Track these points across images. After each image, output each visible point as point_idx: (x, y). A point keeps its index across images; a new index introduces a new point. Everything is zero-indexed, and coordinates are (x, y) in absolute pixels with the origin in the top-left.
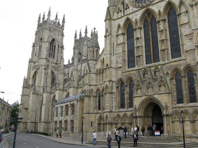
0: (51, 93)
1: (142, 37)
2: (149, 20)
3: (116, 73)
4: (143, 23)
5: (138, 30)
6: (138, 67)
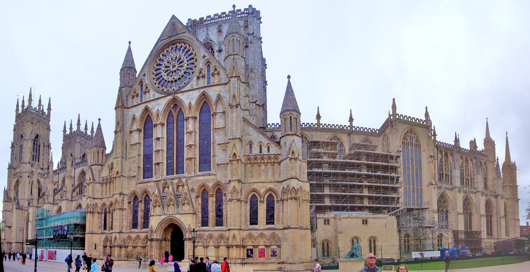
0: (38, 207)
1: (163, 138)
2: (175, 115)
3: (128, 184)
4: (167, 117)
5: (159, 127)
6: (156, 178)
